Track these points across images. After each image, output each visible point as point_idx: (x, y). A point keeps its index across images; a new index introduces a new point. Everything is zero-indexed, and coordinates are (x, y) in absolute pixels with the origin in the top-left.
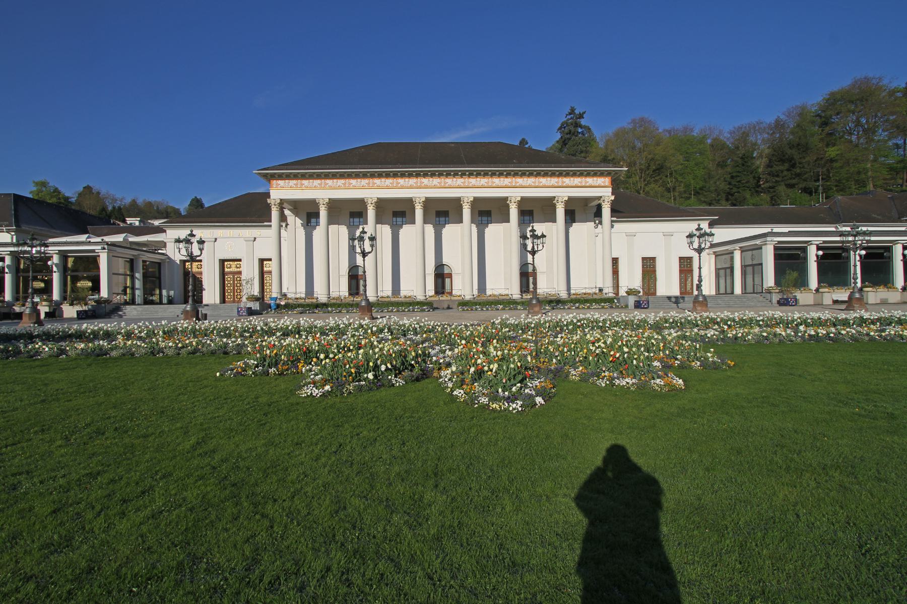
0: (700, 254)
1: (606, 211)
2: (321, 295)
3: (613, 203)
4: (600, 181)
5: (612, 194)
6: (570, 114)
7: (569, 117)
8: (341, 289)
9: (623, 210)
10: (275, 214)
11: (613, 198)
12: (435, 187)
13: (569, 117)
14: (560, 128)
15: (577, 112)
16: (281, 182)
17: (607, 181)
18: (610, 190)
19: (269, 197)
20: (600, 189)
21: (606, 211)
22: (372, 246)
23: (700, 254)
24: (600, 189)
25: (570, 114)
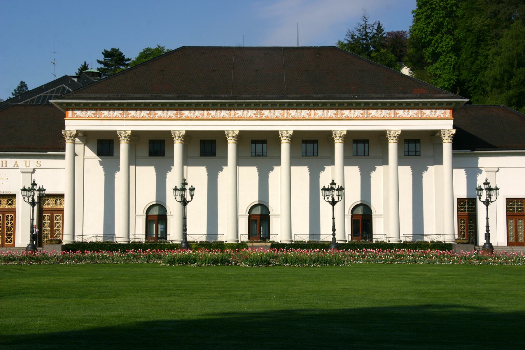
0: (487, 205)
2: (120, 237)
5: (454, 127)
8: (139, 233)
9: (469, 144)
10: (68, 146)
11: (454, 132)
12: (250, 119)
16: (78, 113)
17: (448, 113)
18: (451, 122)
19: (64, 129)
20: (440, 122)
21: (447, 147)
22: (192, 196)
23: (487, 205)
24: (440, 122)
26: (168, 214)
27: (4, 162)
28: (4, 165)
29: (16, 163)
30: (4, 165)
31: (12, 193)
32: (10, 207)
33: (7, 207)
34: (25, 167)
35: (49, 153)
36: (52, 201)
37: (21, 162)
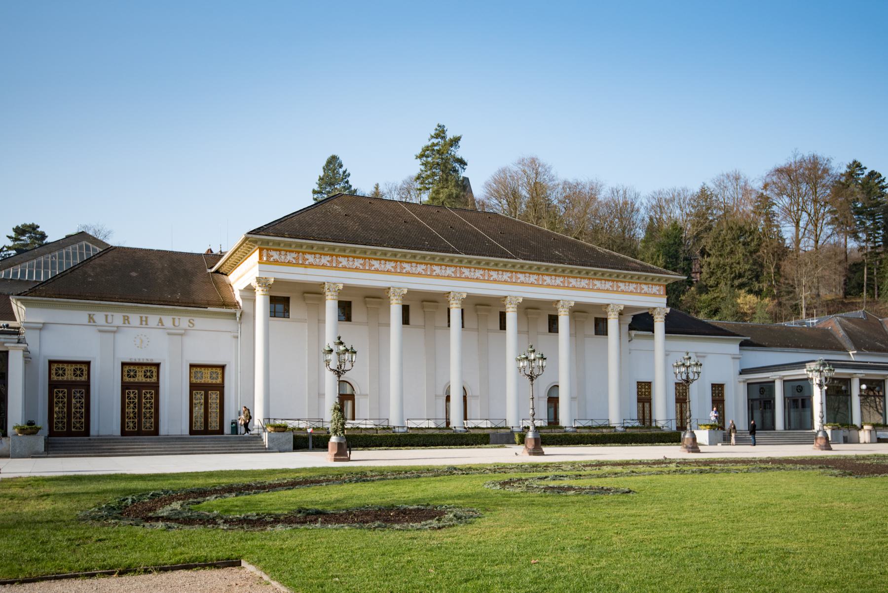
1: (659, 326)
3: (668, 318)
4: (655, 289)
5: (668, 305)
6: (437, 136)
7: (435, 141)
11: (668, 310)
13: (435, 141)
14: (421, 156)
15: (450, 135)
18: (664, 300)
20: (654, 300)
21: (659, 326)
25: (437, 136)
26: (357, 391)
27: (144, 319)
28: (144, 323)
29: (161, 321)
30: (144, 323)
31: (156, 361)
32: (148, 380)
33: (144, 380)
34: (172, 326)
35: (210, 309)
36: (208, 371)
37: (168, 320)
